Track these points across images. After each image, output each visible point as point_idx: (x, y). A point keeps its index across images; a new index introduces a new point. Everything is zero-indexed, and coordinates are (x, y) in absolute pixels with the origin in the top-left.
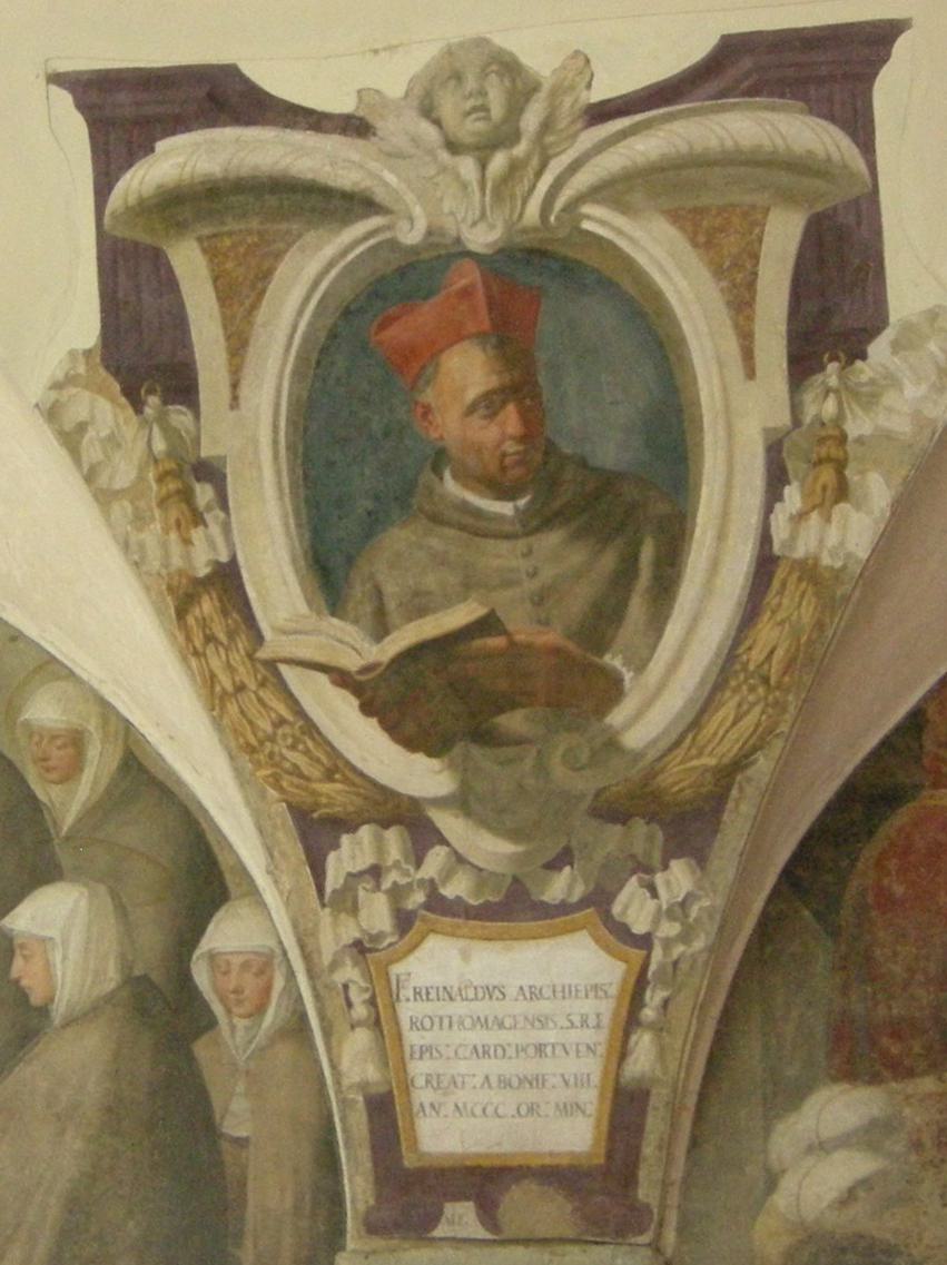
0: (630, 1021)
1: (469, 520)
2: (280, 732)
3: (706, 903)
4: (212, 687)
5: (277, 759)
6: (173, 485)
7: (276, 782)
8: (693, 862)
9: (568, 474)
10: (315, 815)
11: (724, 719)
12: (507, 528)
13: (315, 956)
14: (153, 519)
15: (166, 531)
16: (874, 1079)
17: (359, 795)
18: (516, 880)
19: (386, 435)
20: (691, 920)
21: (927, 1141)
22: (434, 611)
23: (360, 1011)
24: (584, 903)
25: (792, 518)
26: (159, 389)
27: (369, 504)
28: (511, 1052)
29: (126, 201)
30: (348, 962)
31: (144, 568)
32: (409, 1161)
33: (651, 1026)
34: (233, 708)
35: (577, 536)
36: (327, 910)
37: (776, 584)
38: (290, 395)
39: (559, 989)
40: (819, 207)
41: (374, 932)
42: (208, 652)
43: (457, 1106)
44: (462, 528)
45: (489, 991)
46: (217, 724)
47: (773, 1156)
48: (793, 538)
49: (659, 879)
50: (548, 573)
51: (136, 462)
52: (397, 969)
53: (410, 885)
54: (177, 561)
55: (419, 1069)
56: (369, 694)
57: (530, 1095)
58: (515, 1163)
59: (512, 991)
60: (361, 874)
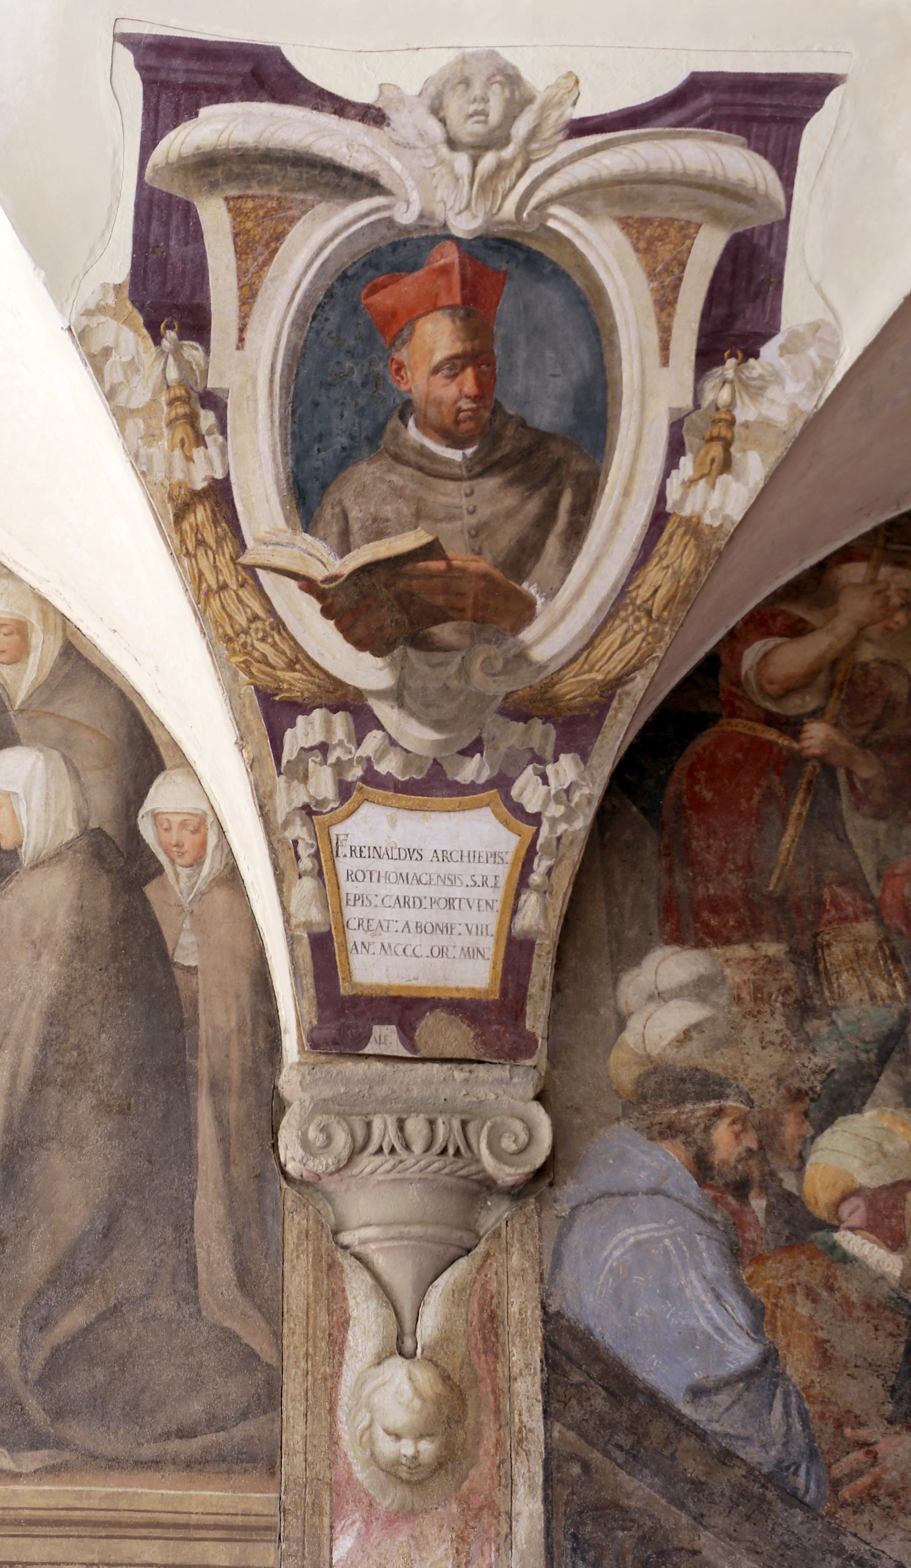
0: (522, 883)
1: (424, 462)
2: (253, 626)
3: (586, 791)
5: (249, 648)
6: (181, 410)
8: (578, 757)
9: (509, 432)
10: (277, 698)
11: (612, 644)
12: (456, 471)
13: (271, 815)
17: (313, 683)
18: (435, 760)
19: (364, 385)
20: (573, 804)
22: (389, 535)
23: (306, 863)
24: (490, 784)
25: (683, 483)
27: (344, 440)
28: (426, 903)
29: (167, 157)
30: (298, 821)
31: (149, 478)
32: (345, 989)
33: (537, 889)
34: (215, 603)
35: (511, 483)
36: (283, 777)
38: (288, 341)
39: (465, 854)
40: (740, 229)
41: (319, 798)
42: (199, 554)
43: (383, 946)
44: (420, 469)
45: (410, 853)
47: (622, 1001)
49: (550, 769)
50: (484, 512)
51: (151, 385)
52: (335, 830)
53: (351, 760)
54: (178, 475)
55: (352, 913)
56: (329, 601)
57: (442, 940)
58: (430, 995)
59: (428, 854)
60: (312, 749)
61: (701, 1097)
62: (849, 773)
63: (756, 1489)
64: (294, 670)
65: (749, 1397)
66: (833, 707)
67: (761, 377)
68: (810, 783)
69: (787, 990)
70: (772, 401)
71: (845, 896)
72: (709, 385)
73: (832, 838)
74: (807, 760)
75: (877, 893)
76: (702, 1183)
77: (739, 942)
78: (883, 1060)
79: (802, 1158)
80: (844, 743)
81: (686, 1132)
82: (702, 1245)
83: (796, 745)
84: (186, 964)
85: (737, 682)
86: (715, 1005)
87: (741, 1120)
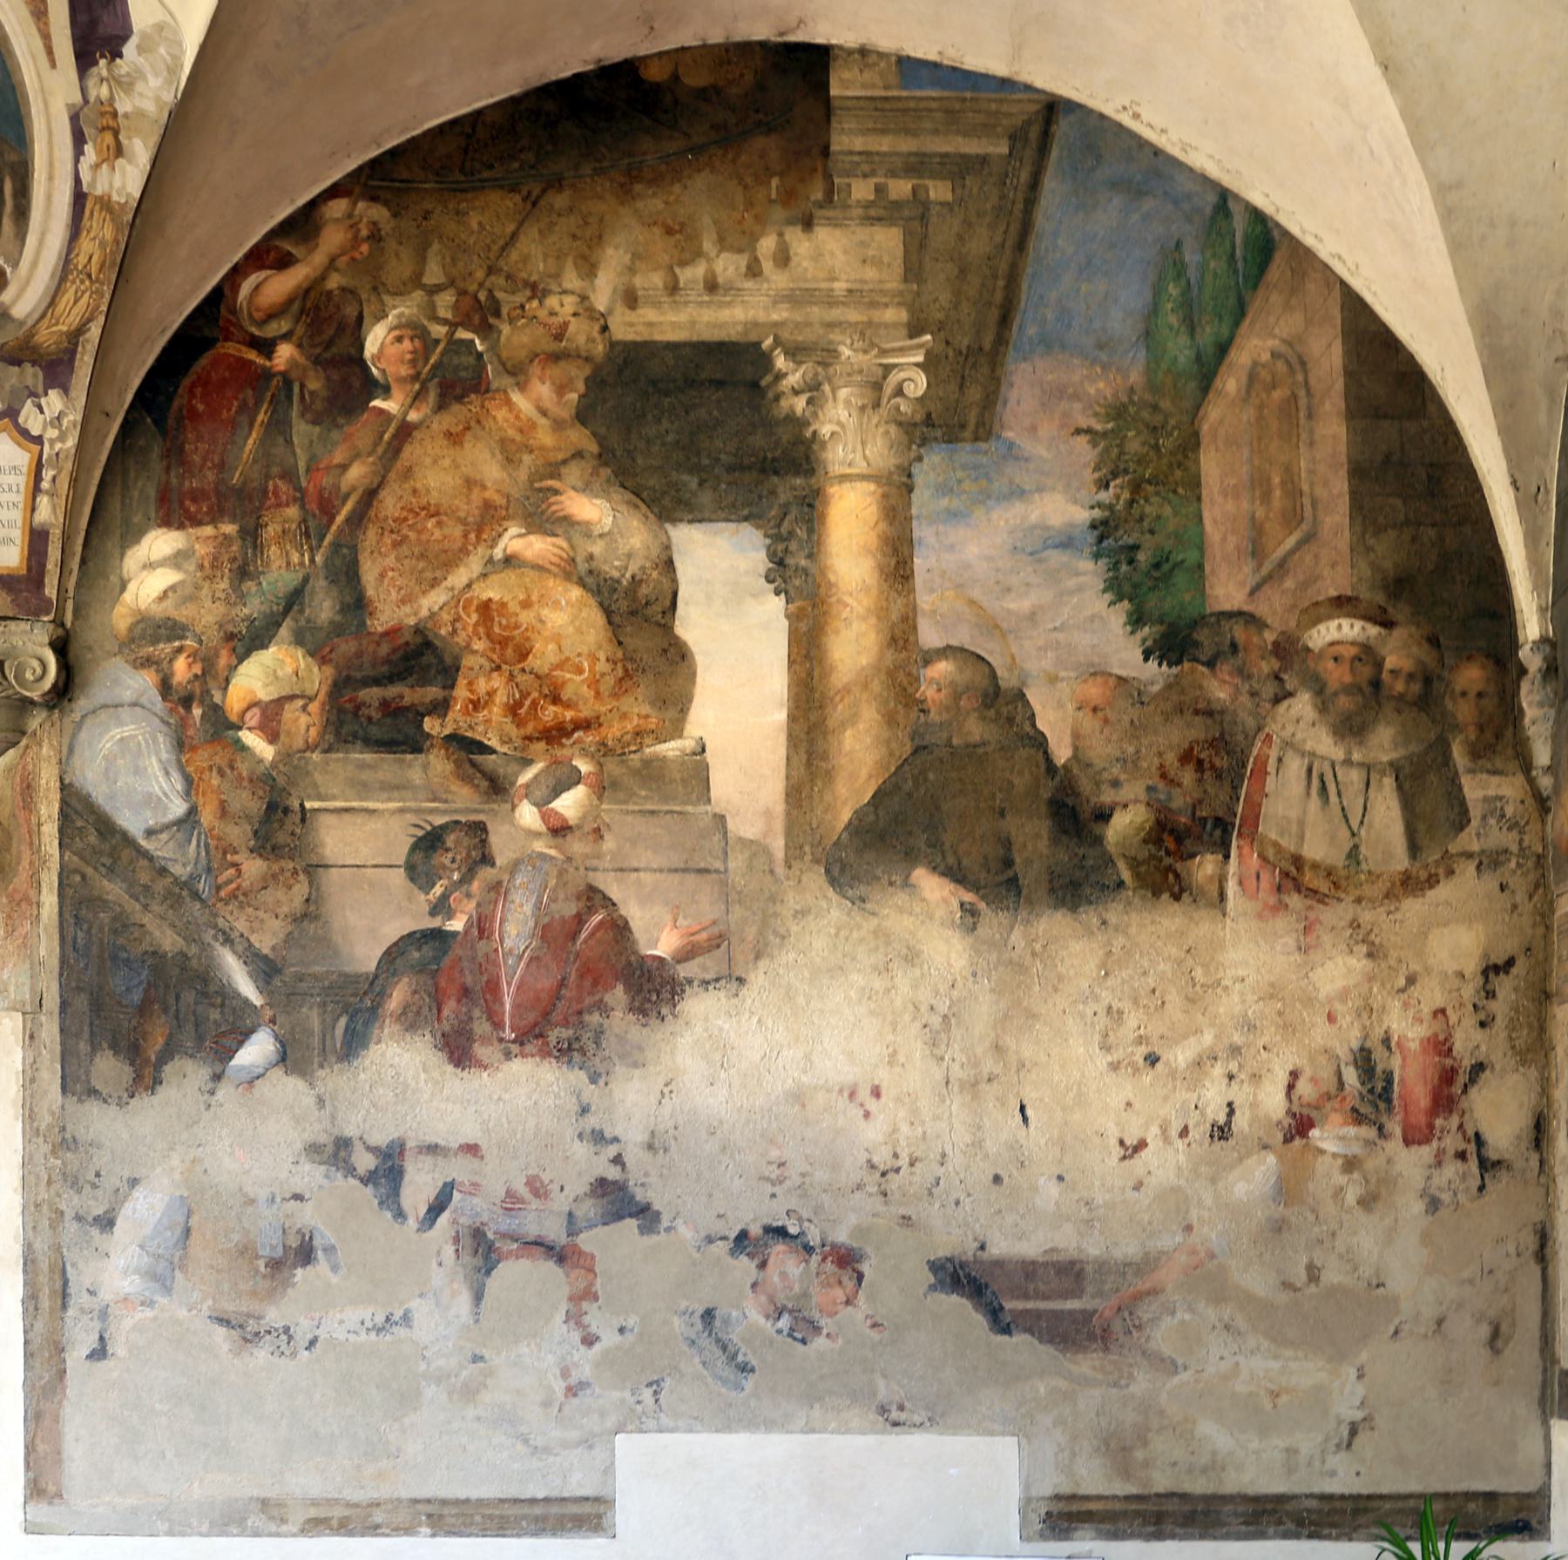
16: (181, 527)
21: (206, 564)
33: (47, 492)
37: (87, 212)
48: (94, 180)
61: (169, 639)
62: (302, 386)
63: (177, 890)
65: (179, 835)
66: (300, 330)
67: (128, 74)
68: (273, 395)
69: (235, 559)
70: (141, 95)
71: (283, 486)
72: (91, 83)
73: (281, 440)
74: (274, 375)
75: (304, 484)
76: (164, 698)
77: (207, 524)
78: (287, 610)
79: (227, 681)
80: (302, 360)
81: (157, 663)
82: (161, 739)
83: (268, 364)
85: (233, 311)
86: (186, 572)
87: (194, 655)
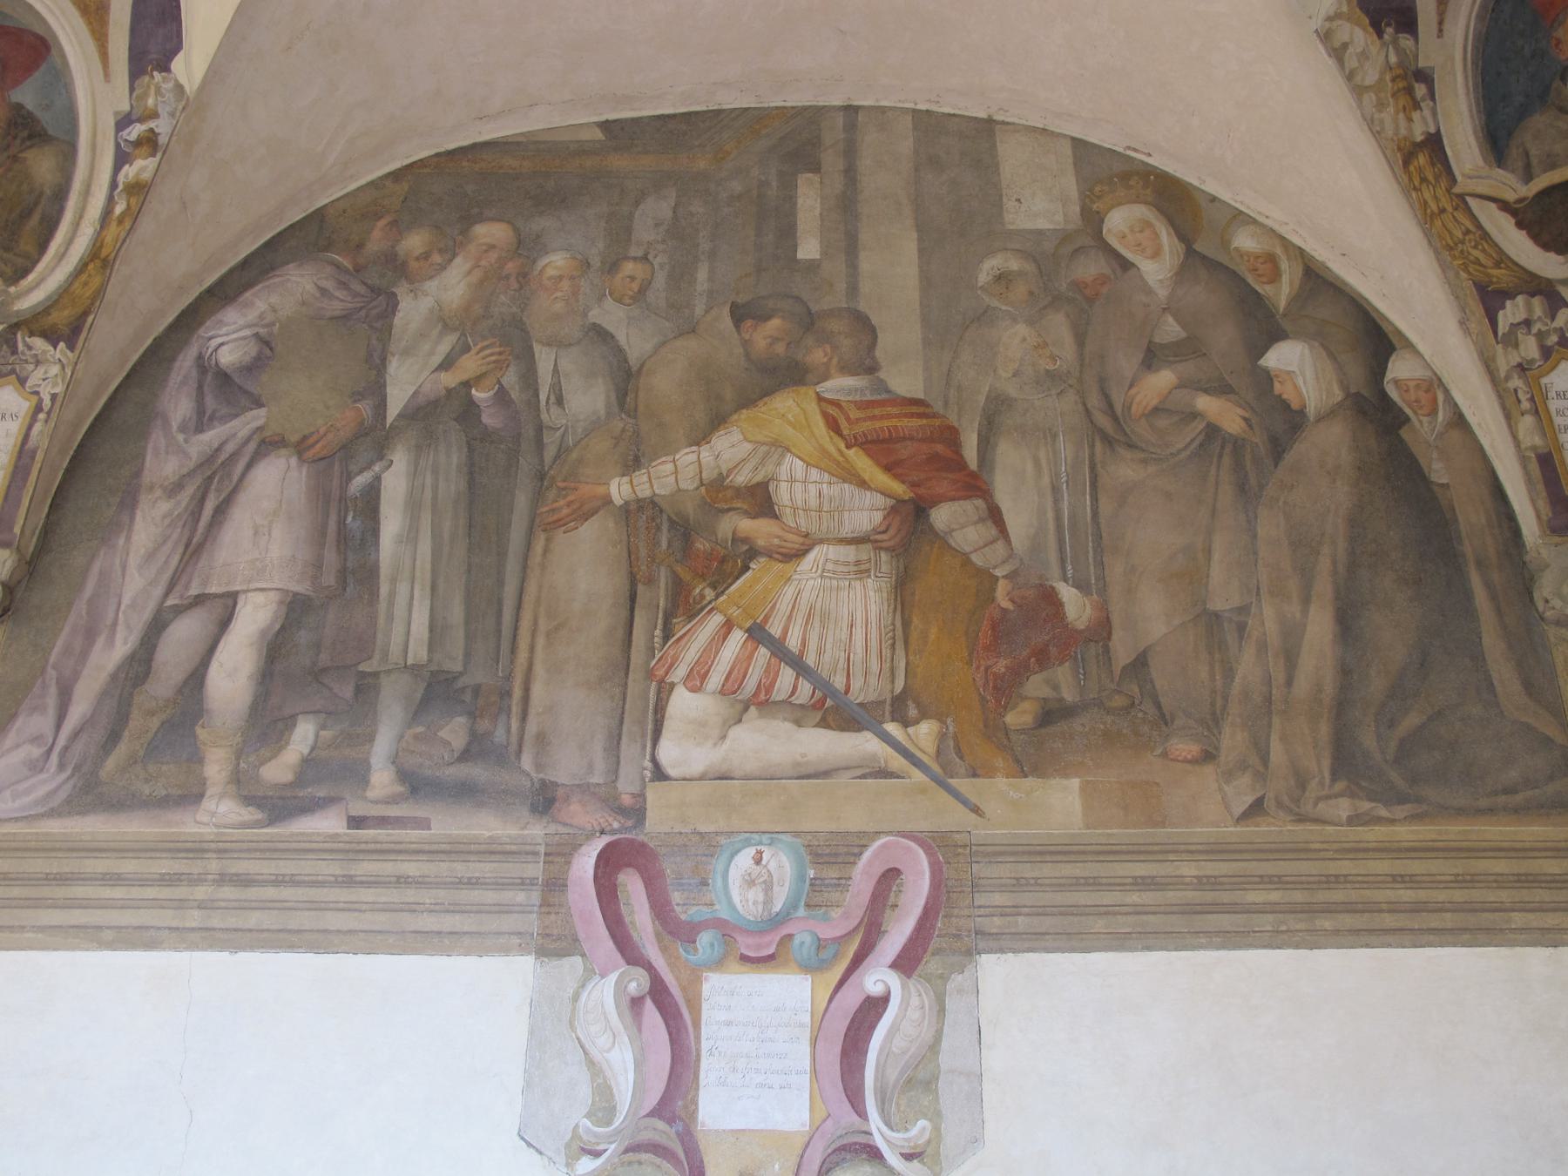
2: (1467, 238)
4: (1425, 210)
7: (1465, 268)
14: (1389, 105)
15: (1397, 112)
17: (1515, 277)
22: (1561, 166)
23: (1526, 405)
26: (1392, 22)
30: (1516, 376)
31: (1383, 135)
34: (1438, 223)
36: (1500, 345)
42: (1423, 189)
46: (1427, 234)
52: (1544, 381)
53: (1548, 331)
54: (1403, 132)
60: (1519, 324)
64: (1500, 268)
84: (1441, 482)
